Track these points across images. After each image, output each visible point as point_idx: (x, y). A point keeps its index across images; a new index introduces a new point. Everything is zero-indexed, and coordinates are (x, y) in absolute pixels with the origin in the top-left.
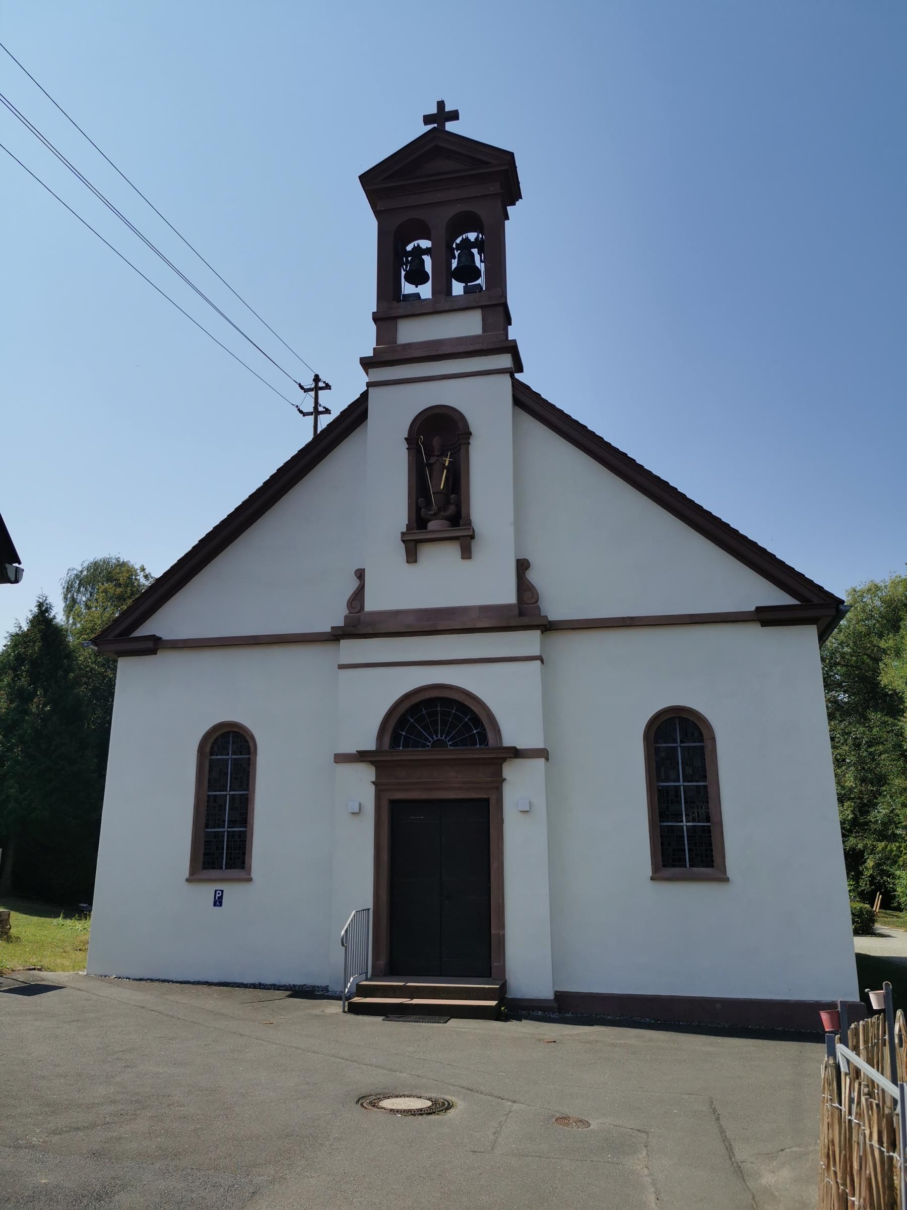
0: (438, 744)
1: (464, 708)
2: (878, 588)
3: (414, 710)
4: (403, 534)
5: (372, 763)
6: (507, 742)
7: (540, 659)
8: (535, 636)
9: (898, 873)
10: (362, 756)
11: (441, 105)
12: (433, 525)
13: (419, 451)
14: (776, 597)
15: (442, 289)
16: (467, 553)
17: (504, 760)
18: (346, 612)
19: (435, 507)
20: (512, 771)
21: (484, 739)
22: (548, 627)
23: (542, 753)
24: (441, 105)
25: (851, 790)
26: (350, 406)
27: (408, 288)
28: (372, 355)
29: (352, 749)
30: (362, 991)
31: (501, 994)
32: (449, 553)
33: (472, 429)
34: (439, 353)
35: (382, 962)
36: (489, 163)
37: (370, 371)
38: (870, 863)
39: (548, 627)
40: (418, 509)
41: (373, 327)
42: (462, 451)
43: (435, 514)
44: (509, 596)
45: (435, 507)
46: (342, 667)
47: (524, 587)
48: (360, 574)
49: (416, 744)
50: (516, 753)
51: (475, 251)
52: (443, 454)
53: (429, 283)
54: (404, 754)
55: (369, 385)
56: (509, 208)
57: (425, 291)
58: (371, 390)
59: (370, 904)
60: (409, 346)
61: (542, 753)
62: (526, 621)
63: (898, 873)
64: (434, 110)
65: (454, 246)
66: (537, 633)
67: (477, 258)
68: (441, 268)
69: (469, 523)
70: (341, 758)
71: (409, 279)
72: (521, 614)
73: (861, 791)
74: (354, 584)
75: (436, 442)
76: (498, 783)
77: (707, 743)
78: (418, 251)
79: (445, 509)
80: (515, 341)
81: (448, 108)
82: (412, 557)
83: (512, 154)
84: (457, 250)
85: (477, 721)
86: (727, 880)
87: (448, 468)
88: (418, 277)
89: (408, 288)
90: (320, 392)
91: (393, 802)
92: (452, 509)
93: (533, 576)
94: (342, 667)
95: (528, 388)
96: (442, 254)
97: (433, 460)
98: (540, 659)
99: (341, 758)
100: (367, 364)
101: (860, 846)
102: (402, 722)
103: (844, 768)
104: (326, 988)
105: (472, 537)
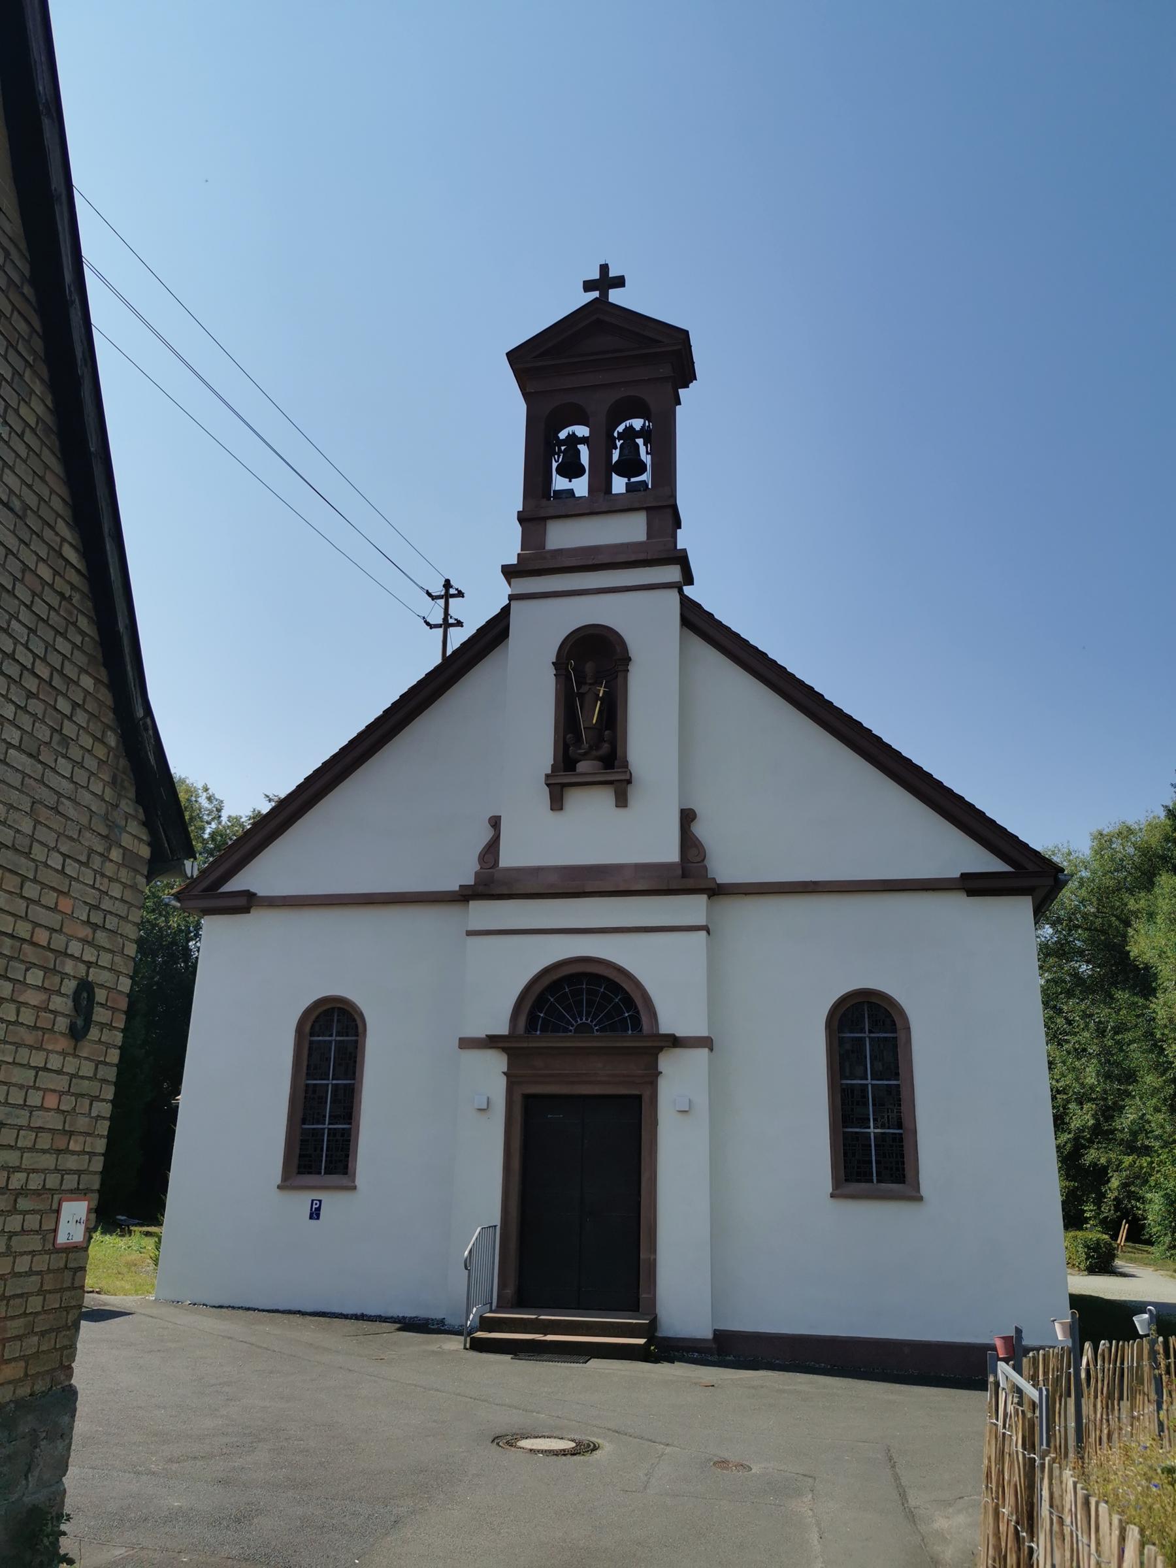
0: (583, 1029)
1: (615, 987)
2: (1130, 831)
3: (555, 986)
4: (547, 776)
5: (504, 1049)
6: (666, 1027)
7: (706, 929)
9: (1149, 1196)
10: (492, 1042)
11: (604, 268)
12: (582, 766)
14: (985, 862)
15: (600, 486)
16: (622, 801)
17: (661, 1049)
18: (477, 867)
19: (586, 745)
20: (670, 1064)
21: (636, 1023)
22: (716, 891)
23: (705, 1042)
24: (604, 268)
25: (1092, 1088)
27: (560, 483)
29: (481, 1033)
30: (486, 1324)
31: (650, 1330)
32: (603, 798)
34: (596, 562)
35: (510, 1291)
37: (513, 581)
38: (1115, 1183)
39: (716, 891)
40: (566, 747)
41: (517, 529)
42: (620, 679)
43: (585, 754)
44: (671, 854)
45: (586, 745)
46: (470, 933)
47: (689, 842)
48: (495, 822)
49: (556, 1029)
50: (675, 1042)
51: (640, 441)
53: (586, 477)
54: (543, 1041)
55: (512, 598)
56: (681, 391)
57: (580, 486)
59: (496, 1220)
61: (705, 1042)
62: (690, 883)
63: (1149, 1196)
64: (595, 275)
65: (616, 434)
66: (703, 898)
69: (625, 764)
70: (467, 1043)
72: (685, 875)
73: (1105, 1091)
74: (487, 835)
75: (589, 668)
76: (653, 1076)
77: (901, 1035)
78: (573, 440)
79: (598, 748)
80: (685, 550)
82: (557, 803)
83: (687, 332)
85: (629, 1002)
86: (920, 1199)
87: (602, 699)
88: (572, 470)
89: (560, 483)
90: (451, 600)
91: (527, 1098)
92: (606, 747)
93: (700, 830)
94: (470, 933)
95: (699, 606)
96: (601, 443)
97: (584, 689)
98: (706, 929)
99: (467, 1043)
100: (509, 572)
101: (1103, 1161)
103: (1083, 1060)
104: (442, 1321)
105: (629, 782)
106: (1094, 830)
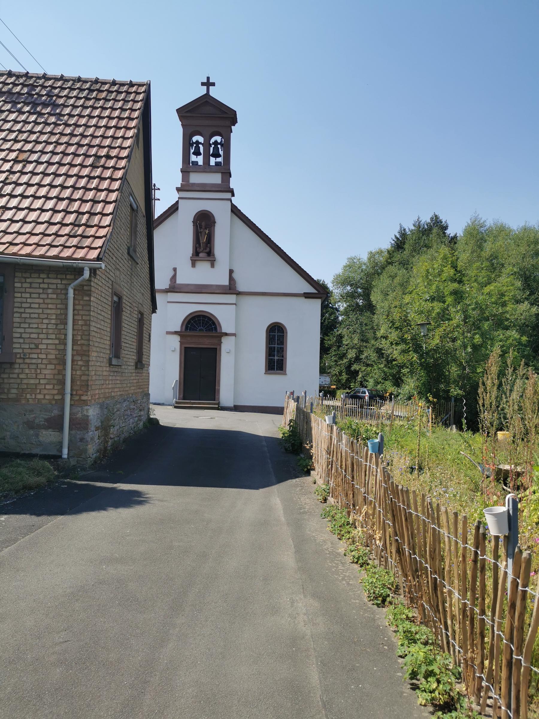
0: (201, 330)
1: (210, 319)
2: (382, 252)
3: (193, 318)
4: (191, 257)
5: (179, 335)
6: (224, 330)
7: (235, 304)
8: (234, 296)
9: (370, 380)
10: (176, 333)
11: (208, 78)
12: (201, 255)
13: (197, 226)
14: (310, 289)
15: (206, 161)
16: (213, 266)
17: (222, 336)
18: (169, 283)
19: (202, 248)
20: (224, 340)
21: (216, 329)
22: (239, 294)
23: (234, 335)
24: (208, 78)
25: (356, 344)
26: (172, 206)
27: (193, 158)
28: (180, 186)
29: (173, 330)
30: (177, 403)
31: (218, 404)
32: (207, 265)
33: (216, 221)
34: (205, 189)
35: (182, 396)
36: (227, 113)
37: (179, 192)
38: (360, 376)
39: (239, 294)
40: (196, 248)
41: (180, 175)
42: (212, 228)
43: (202, 251)
44: (226, 283)
45: (202, 248)
46: (168, 302)
47: (231, 279)
48: (175, 270)
49: (193, 330)
50: (226, 334)
51: (219, 146)
52: (206, 228)
53: (202, 156)
54: (189, 333)
55: (179, 198)
56: (232, 127)
57: (200, 160)
58: (180, 200)
59: (178, 379)
60: (194, 184)
61: (234, 335)
62: (231, 291)
63: (370, 380)
64: (205, 81)
65: (211, 142)
66: (235, 296)
67: (220, 150)
68: (206, 150)
69: (214, 255)
70: (168, 333)
71: (194, 153)
72: (230, 289)
73: (360, 346)
74: (172, 273)
75: (203, 224)
76: (220, 343)
77: (285, 334)
78: (198, 143)
79: (206, 249)
80: (233, 189)
81: (211, 81)
82: (193, 265)
83: (236, 112)
84: (213, 144)
85: (214, 323)
86: (286, 374)
87: (207, 235)
88: (197, 153)
89: (193, 158)
90: (156, 191)
91: (185, 348)
92: (208, 250)
93: (234, 275)
94: (168, 302)
95: (236, 207)
96: (207, 145)
97: (202, 230)
98: (235, 304)
99: (168, 333)
100: (178, 190)
101: (357, 369)
102: (189, 322)
103: (354, 335)
104: (163, 403)
105: (215, 260)
106: (369, 251)
